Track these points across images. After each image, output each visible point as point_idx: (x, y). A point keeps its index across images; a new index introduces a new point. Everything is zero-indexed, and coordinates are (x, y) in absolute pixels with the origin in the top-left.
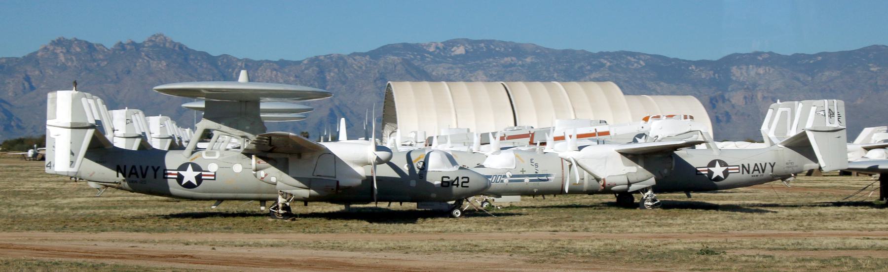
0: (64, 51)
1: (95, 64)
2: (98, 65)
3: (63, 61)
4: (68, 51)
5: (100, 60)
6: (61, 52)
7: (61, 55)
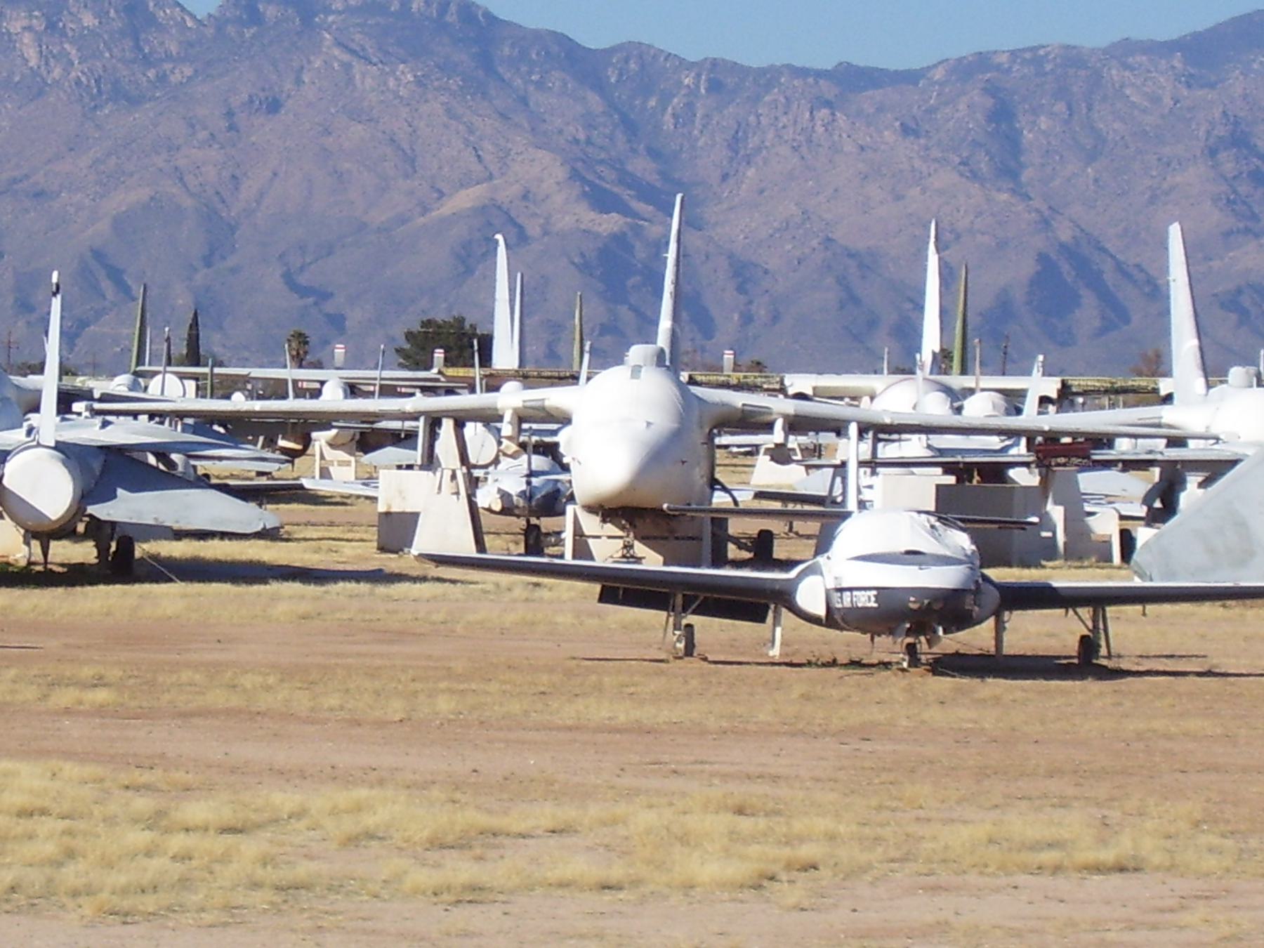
0: (39, 25)
1: (151, 74)
2: (162, 78)
3: (32, 63)
4: (51, 26)
5: (169, 57)
6: (29, 28)
7: (27, 38)
